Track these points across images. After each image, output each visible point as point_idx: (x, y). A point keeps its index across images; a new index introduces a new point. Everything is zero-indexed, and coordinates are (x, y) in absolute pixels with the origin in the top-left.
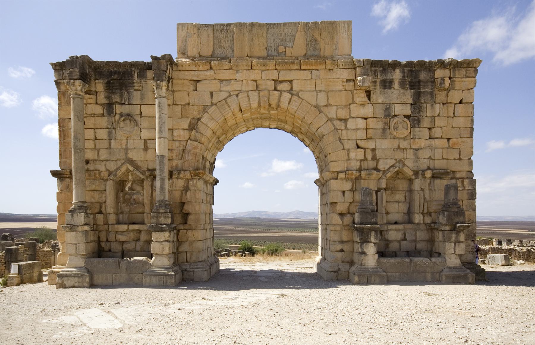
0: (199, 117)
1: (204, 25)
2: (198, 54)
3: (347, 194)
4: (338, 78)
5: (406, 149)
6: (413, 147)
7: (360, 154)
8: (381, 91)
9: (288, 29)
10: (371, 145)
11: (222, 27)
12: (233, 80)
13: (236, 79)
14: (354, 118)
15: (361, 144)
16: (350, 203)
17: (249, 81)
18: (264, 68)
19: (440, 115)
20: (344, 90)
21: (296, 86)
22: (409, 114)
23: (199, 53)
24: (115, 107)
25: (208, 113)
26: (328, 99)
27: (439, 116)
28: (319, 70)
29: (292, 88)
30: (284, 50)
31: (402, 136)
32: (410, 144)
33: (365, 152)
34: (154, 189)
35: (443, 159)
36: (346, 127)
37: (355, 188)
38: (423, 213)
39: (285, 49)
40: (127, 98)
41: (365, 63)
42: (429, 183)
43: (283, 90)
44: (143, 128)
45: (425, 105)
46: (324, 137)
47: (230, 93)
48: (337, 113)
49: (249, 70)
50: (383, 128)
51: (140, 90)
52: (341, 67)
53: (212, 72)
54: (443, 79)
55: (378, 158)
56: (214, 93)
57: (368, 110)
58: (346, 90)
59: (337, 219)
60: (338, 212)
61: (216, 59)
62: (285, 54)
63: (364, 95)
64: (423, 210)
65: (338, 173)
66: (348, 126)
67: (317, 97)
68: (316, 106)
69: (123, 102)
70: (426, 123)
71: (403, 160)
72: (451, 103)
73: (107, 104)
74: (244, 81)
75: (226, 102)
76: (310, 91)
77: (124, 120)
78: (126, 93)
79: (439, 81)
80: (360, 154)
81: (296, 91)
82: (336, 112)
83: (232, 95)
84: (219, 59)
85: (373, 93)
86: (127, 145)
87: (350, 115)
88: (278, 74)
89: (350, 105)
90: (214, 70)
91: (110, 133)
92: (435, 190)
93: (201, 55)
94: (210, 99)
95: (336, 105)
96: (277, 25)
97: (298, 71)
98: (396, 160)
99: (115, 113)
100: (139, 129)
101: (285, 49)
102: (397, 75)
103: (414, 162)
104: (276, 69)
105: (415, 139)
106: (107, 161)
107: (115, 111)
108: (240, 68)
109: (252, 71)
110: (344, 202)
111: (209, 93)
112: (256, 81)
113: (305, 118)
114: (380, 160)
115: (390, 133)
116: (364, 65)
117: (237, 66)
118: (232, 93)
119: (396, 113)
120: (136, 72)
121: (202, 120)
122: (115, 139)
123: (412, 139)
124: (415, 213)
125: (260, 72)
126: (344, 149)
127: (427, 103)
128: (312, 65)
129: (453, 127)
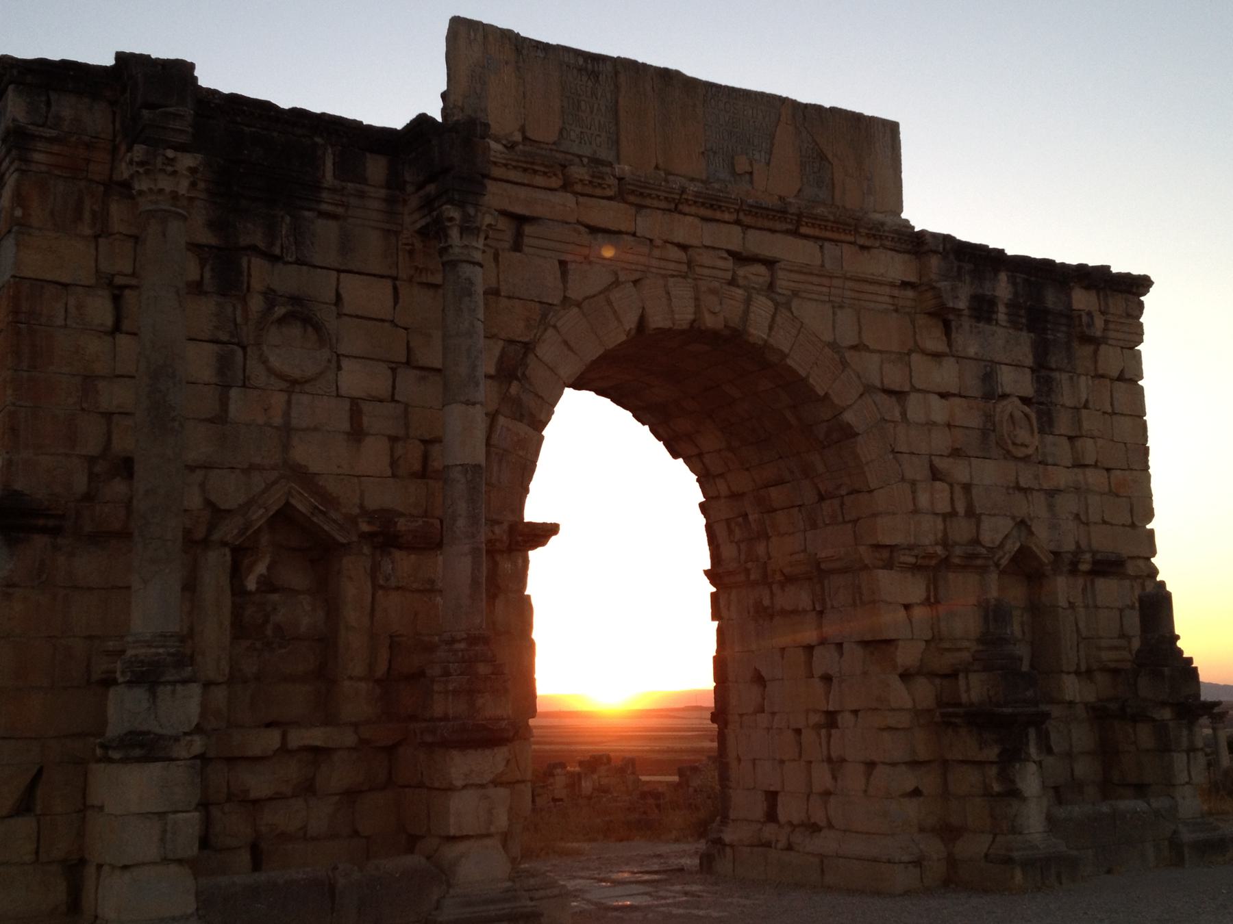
0: (526, 340)
1: (534, 44)
2: (519, 130)
3: (919, 613)
4: (882, 275)
5: (1030, 489)
6: (1045, 486)
7: (941, 498)
8: (971, 326)
9: (755, 112)
10: (960, 471)
11: (581, 61)
12: (627, 233)
13: (634, 235)
14: (919, 391)
15: (942, 464)
16: (926, 641)
17: (669, 246)
18: (708, 213)
19: (1091, 405)
20: (893, 310)
21: (784, 282)
22: (1031, 396)
23: (522, 130)
24: (245, 265)
25: (558, 331)
26: (860, 333)
27: (1086, 407)
28: (839, 244)
29: (771, 286)
30: (748, 168)
31: (1020, 453)
32: (1036, 477)
33: (952, 493)
34: (381, 587)
35: (1104, 522)
36: (904, 414)
37: (936, 596)
38: (1077, 673)
39: (751, 164)
40: (291, 239)
41: (948, 246)
42: (1083, 589)
43: (754, 288)
44: (347, 356)
45: (1056, 375)
46: (860, 437)
47: (616, 274)
48: (882, 373)
49: (670, 210)
50: (981, 427)
51: (334, 217)
52: (888, 243)
53: (569, 199)
54: (1089, 314)
55: (978, 511)
56: (571, 267)
57: (946, 375)
58: (896, 311)
59: (900, 695)
60: (900, 670)
61: (577, 160)
62: (751, 182)
63: (938, 332)
64: (1078, 665)
65: (892, 548)
66: (910, 415)
67: (834, 321)
68: (833, 346)
69: (277, 251)
70: (1063, 424)
71: (1027, 520)
72: (1102, 376)
73: (211, 247)
74: (658, 242)
75: (609, 303)
76: (816, 300)
77: (281, 321)
78: (288, 219)
79: (1085, 319)
80: (941, 498)
81: (783, 295)
82: (881, 369)
83: (623, 283)
84: (585, 160)
85: (957, 329)
86: (287, 414)
87: (911, 382)
88: (744, 238)
89: (909, 354)
90: (575, 193)
91: (223, 364)
92: (1096, 607)
93: (529, 134)
94: (561, 286)
95: (880, 352)
96: (726, 89)
97: (790, 239)
98: (1013, 518)
99: (245, 286)
100: (335, 358)
101: (751, 164)
102: (1003, 288)
103: (1049, 528)
104: (738, 222)
105: (1047, 464)
106: (208, 467)
107: (245, 279)
108: (648, 202)
109: (676, 216)
110: (912, 639)
111: (557, 263)
112: (684, 247)
113: (811, 380)
114: (983, 517)
115: (997, 443)
116: (944, 249)
117: (641, 194)
118: (622, 279)
119: (1008, 390)
120: (330, 151)
121: (539, 352)
122: (244, 386)
123: (1040, 463)
124: (1062, 672)
125: (697, 221)
126: (903, 479)
127: (1058, 369)
128: (826, 226)
129: (1112, 440)
